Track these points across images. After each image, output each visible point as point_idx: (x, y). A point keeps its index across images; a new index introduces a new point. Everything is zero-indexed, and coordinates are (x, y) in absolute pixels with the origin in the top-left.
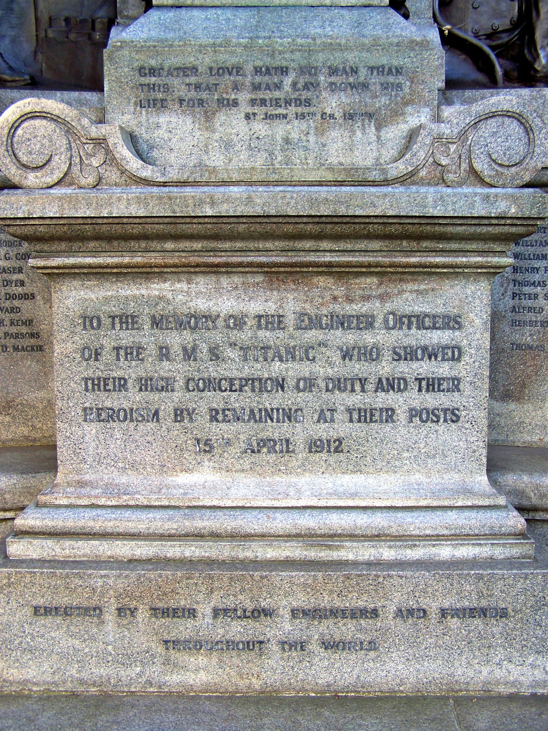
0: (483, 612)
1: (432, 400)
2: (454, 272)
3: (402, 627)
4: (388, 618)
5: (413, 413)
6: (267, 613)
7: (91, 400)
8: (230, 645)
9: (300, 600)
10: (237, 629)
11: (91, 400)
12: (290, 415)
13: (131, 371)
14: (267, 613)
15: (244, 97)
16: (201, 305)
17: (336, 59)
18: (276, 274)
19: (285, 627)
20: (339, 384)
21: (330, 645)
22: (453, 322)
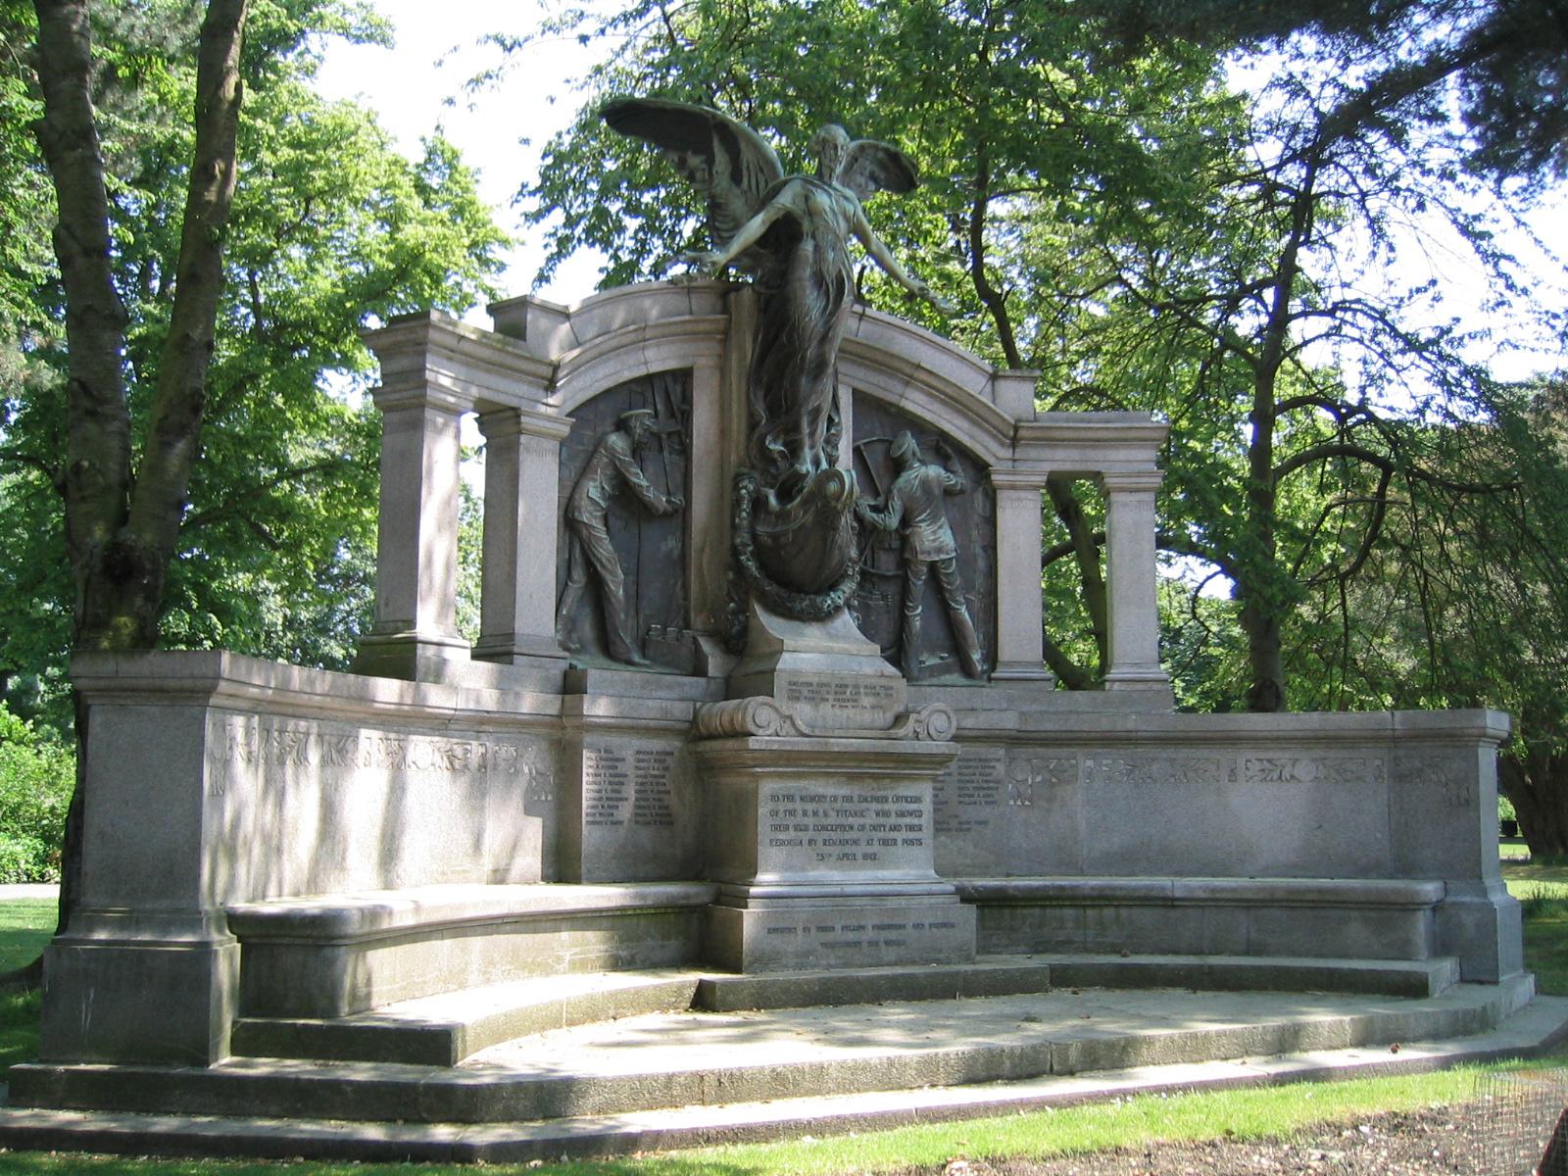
0: (944, 925)
1: (912, 835)
5: (905, 841)
6: (863, 927)
9: (876, 921)
10: (851, 936)
12: (855, 842)
13: (791, 821)
14: (863, 927)
15: (831, 697)
16: (821, 791)
17: (868, 682)
18: (851, 777)
19: (870, 934)
20: (874, 828)
22: (918, 800)
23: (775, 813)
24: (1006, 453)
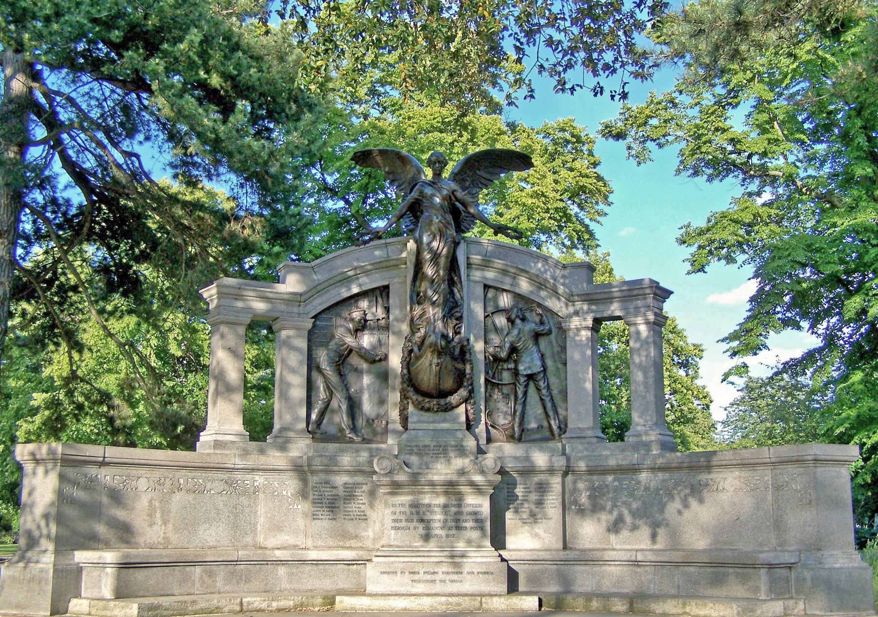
0: (488, 573)
3: (469, 577)
4: (465, 575)
6: (436, 573)
7: (393, 524)
8: (427, 581)
11: (393, 524)
14: (436, 573)
19: (440, 576)
21: (452, 581)
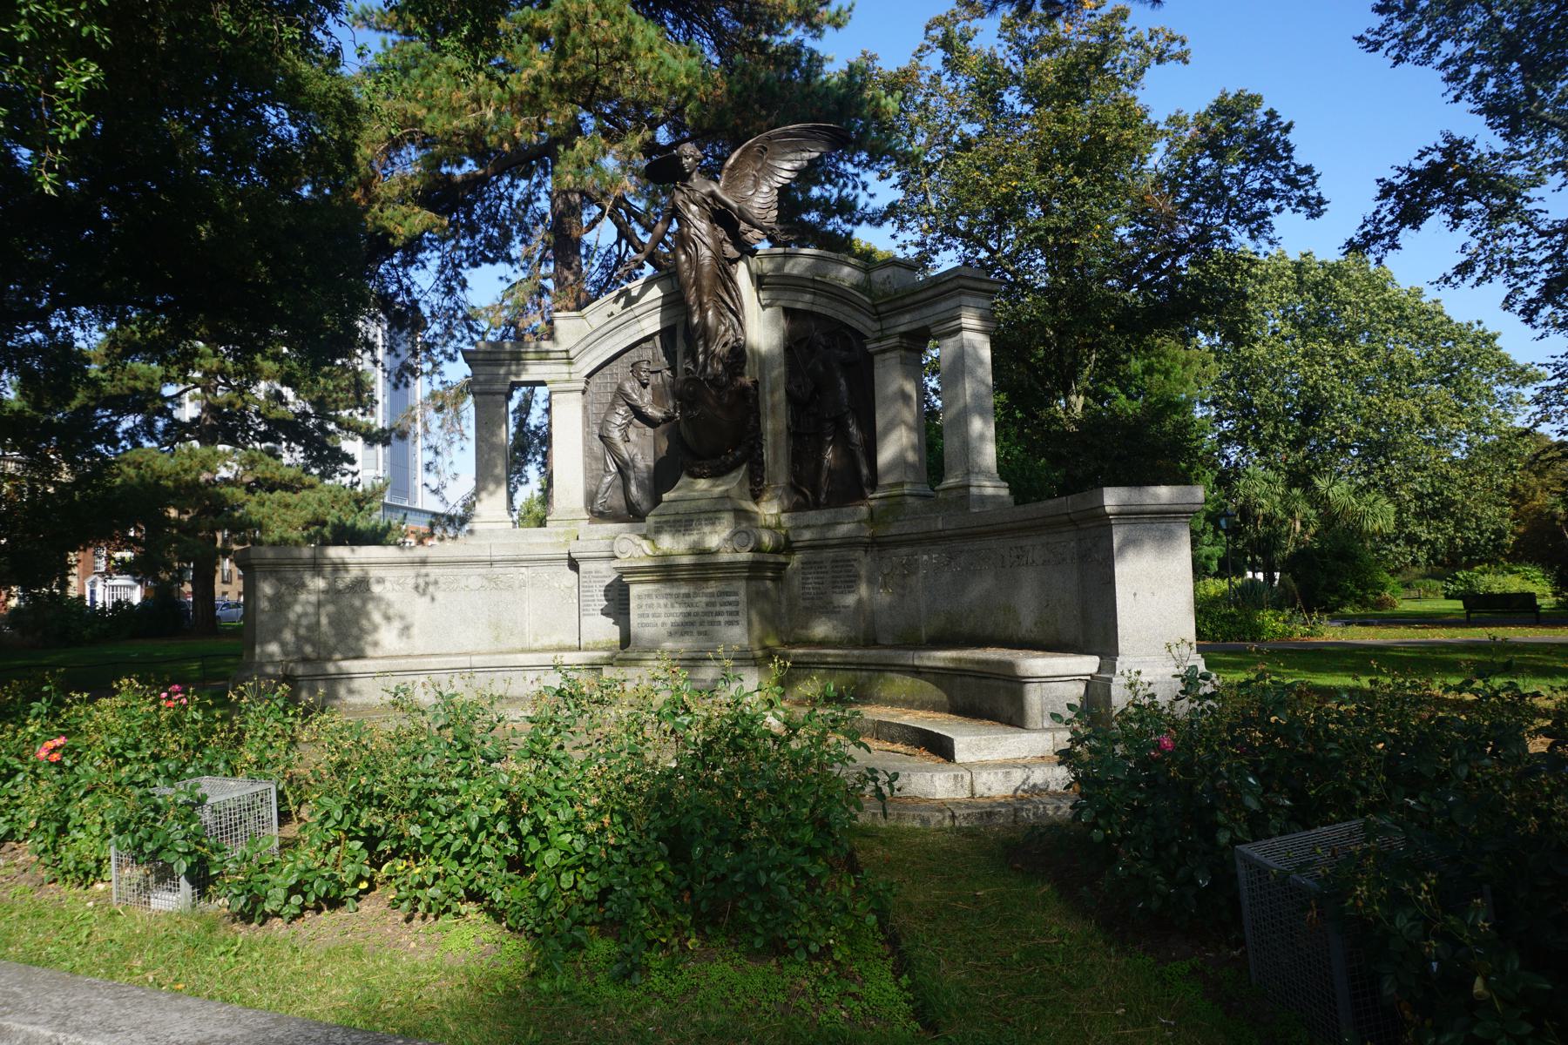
2: (734, 578)
13: (650, 611)
23: (640, 607)
24: (877, 326)
